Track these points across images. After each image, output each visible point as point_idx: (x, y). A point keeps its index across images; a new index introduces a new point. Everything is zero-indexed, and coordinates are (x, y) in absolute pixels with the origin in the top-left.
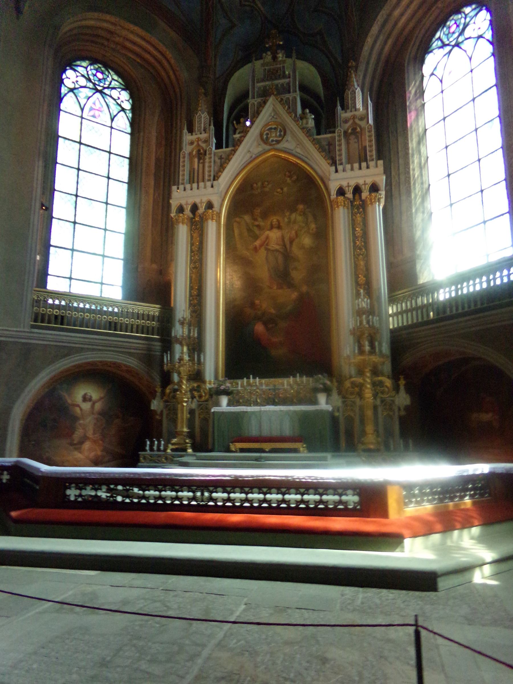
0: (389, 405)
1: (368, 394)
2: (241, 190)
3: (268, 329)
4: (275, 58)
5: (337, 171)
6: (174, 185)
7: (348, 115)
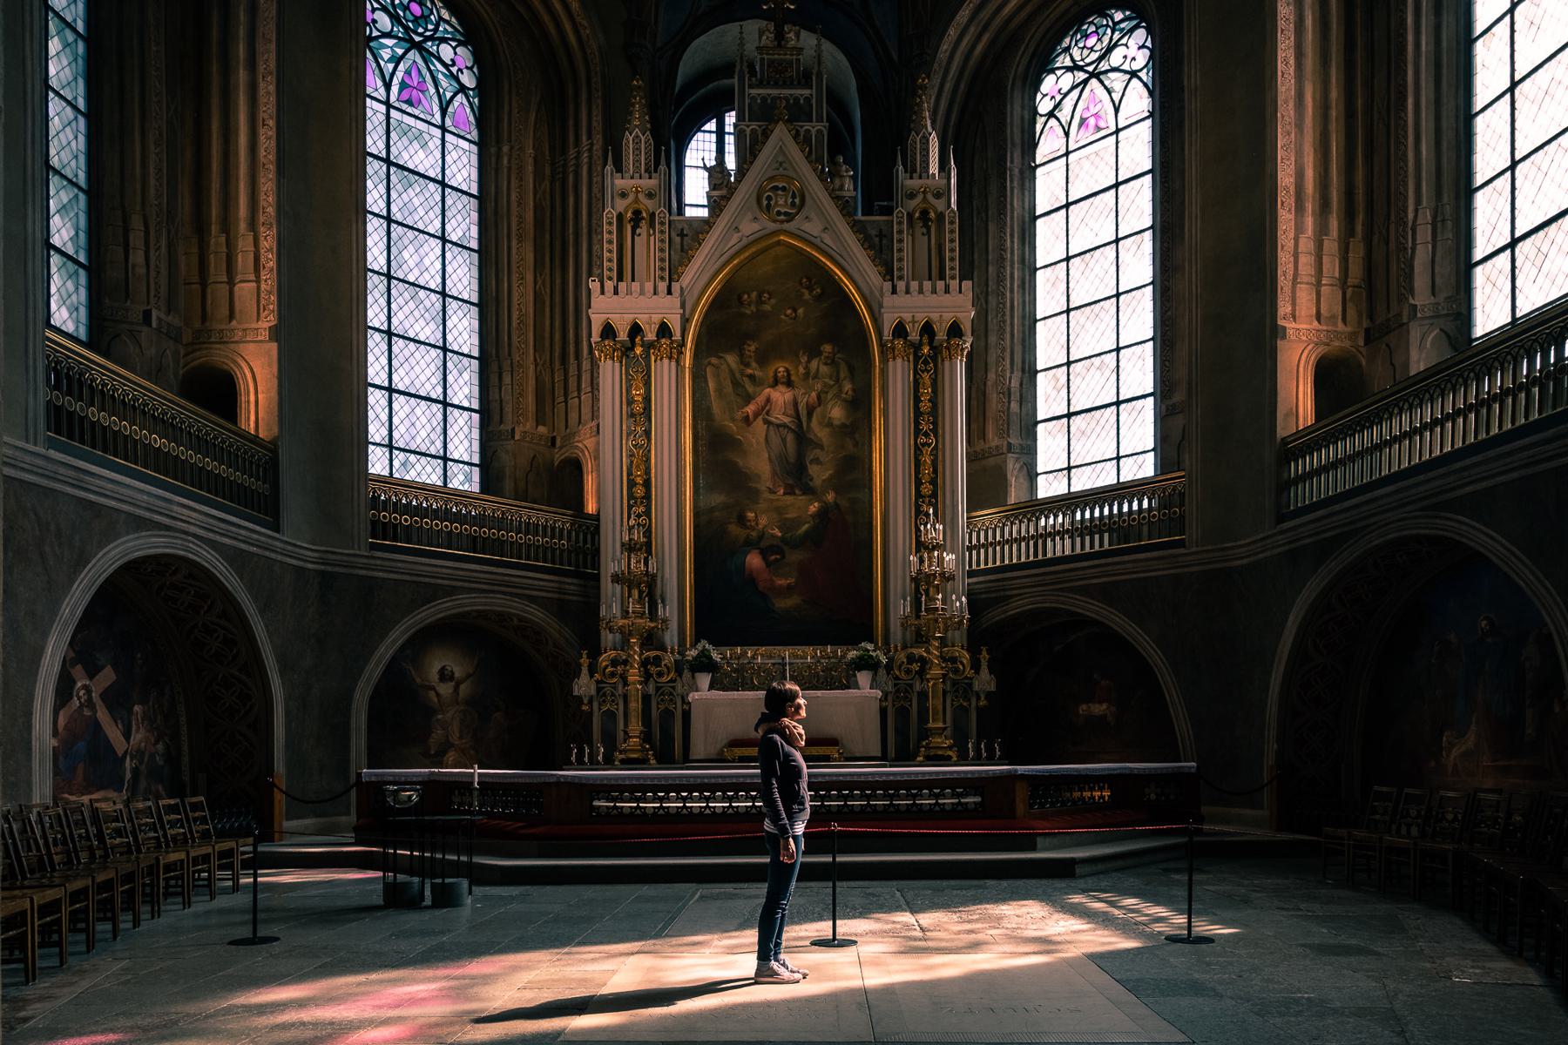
2: (717, 304)
4: (780, 36)
5: (894, 291)
6: (590, 275)
7: (914, 183)
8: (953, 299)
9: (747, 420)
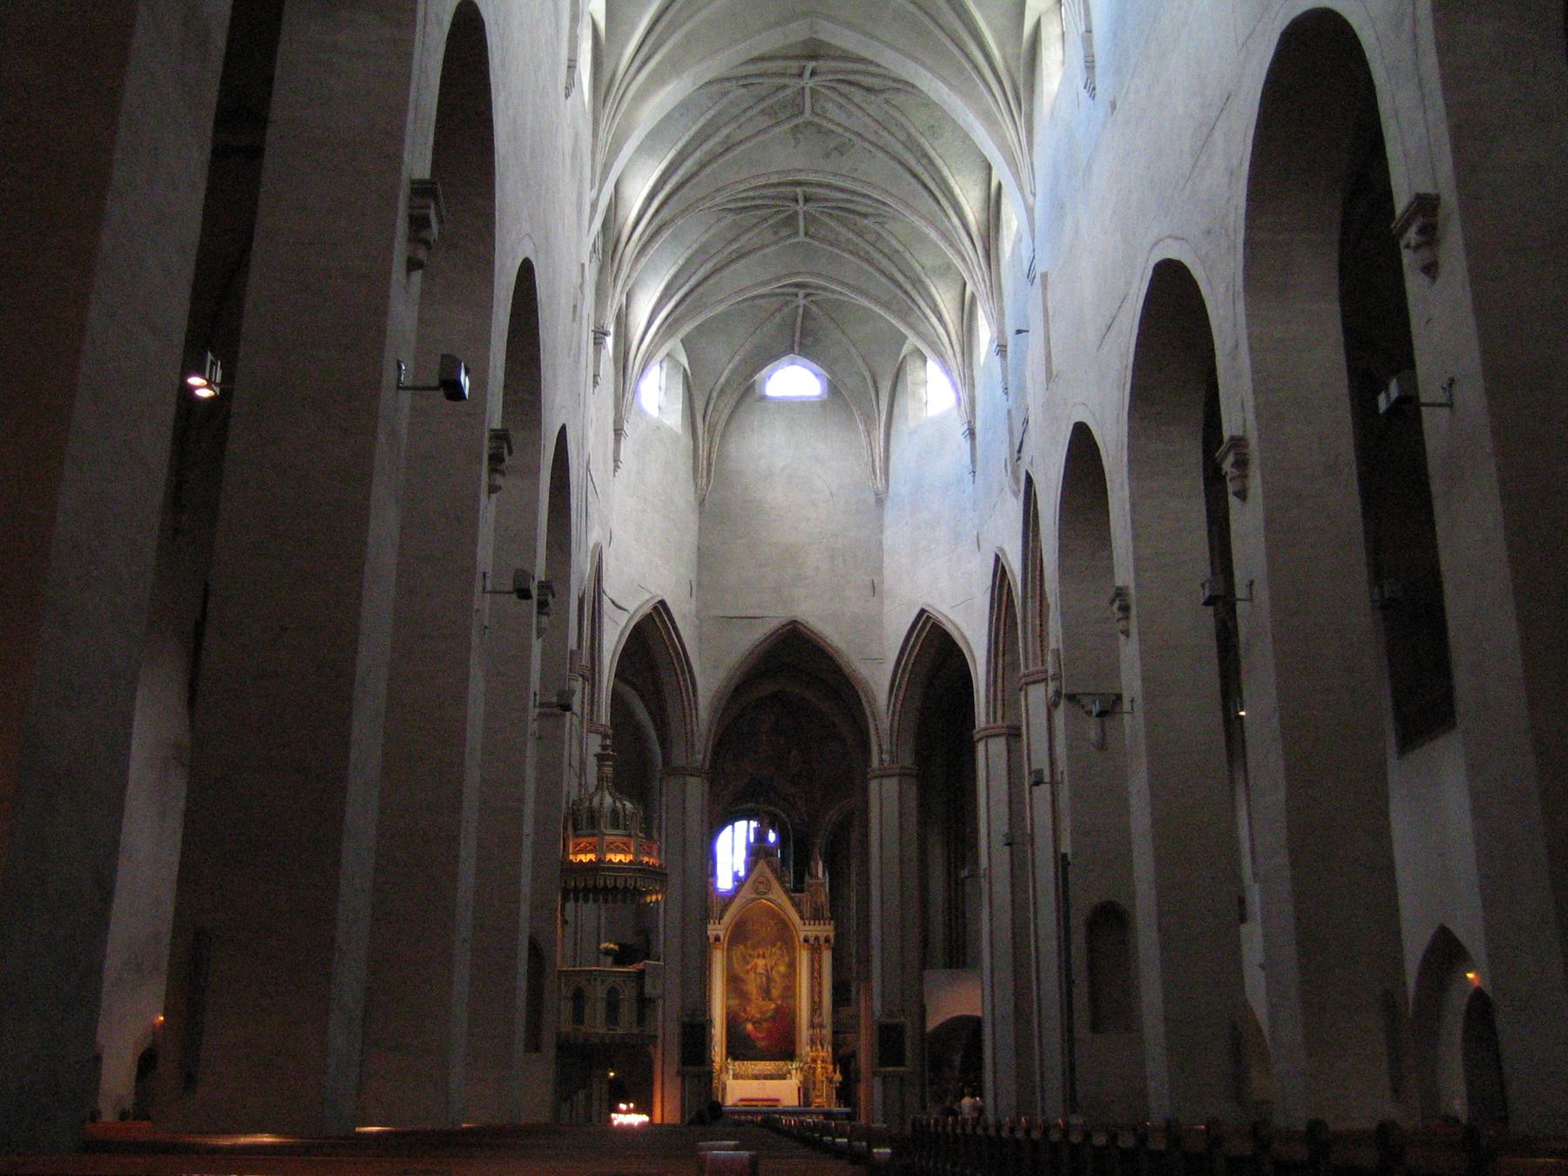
0: (831, 1081)
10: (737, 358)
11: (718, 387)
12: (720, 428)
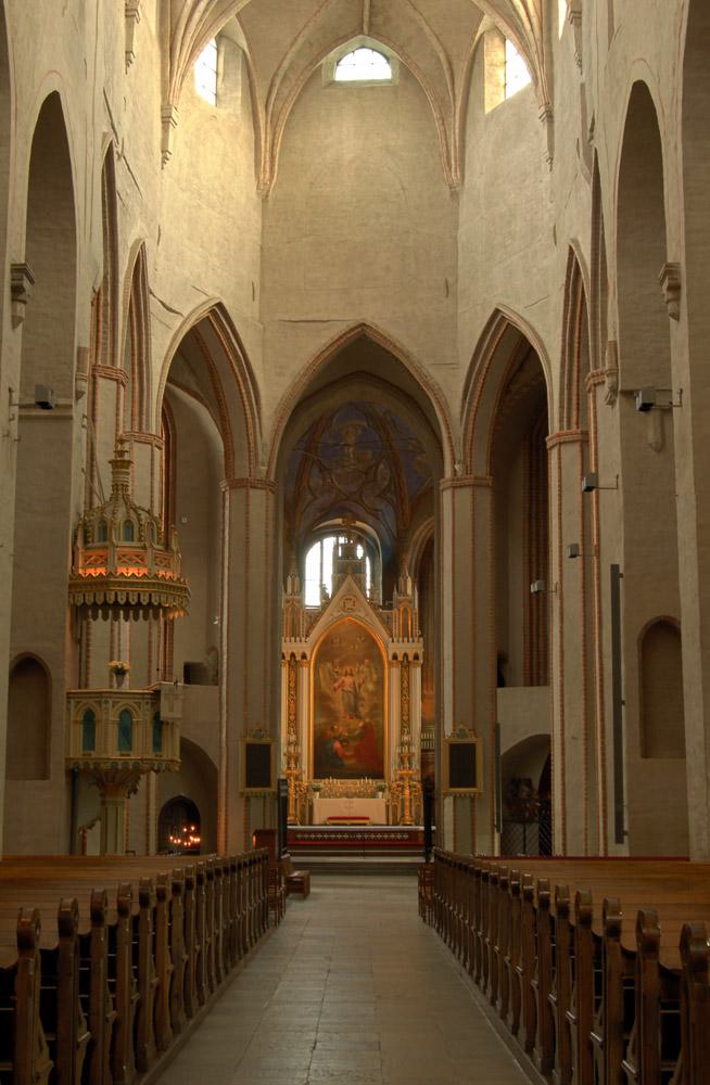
1: (407, 792)
2: (324, 643)
3: (343, 746)
8: (414, 645)
9: (335, 689)
10: (301, 40)
11: (281, 73)
12: (285, 117)
